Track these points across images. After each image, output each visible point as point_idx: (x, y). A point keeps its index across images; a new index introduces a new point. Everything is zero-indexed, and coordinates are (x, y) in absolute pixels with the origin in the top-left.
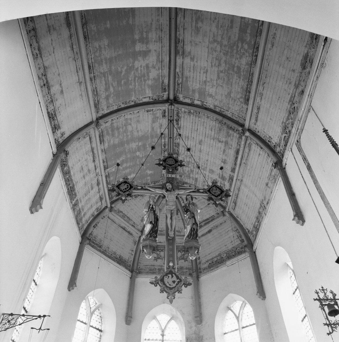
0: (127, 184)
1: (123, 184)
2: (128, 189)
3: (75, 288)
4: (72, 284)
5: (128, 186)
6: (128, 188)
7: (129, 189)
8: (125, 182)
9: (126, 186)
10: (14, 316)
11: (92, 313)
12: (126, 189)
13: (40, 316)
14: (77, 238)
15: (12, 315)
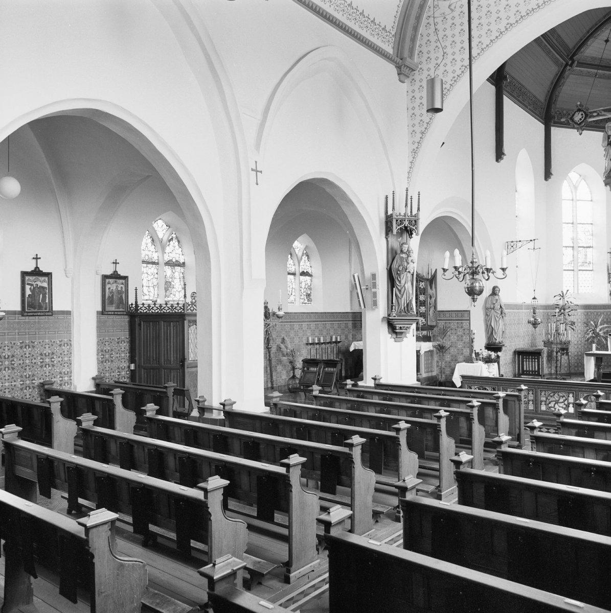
0: (581, 113)
1: (577, 113)
2: (583, 119)
3: (552, 177)
4: (548, 174)
5: (582, 114)
6: (582, 117)
7: (585, 119)
8: (579, 110)
9: (580, 116)
10: (514, 243)
11: (576, 188)
12: (581, 119)
13: (531, 240)
14: (541, 127)
15: (512, 242)
